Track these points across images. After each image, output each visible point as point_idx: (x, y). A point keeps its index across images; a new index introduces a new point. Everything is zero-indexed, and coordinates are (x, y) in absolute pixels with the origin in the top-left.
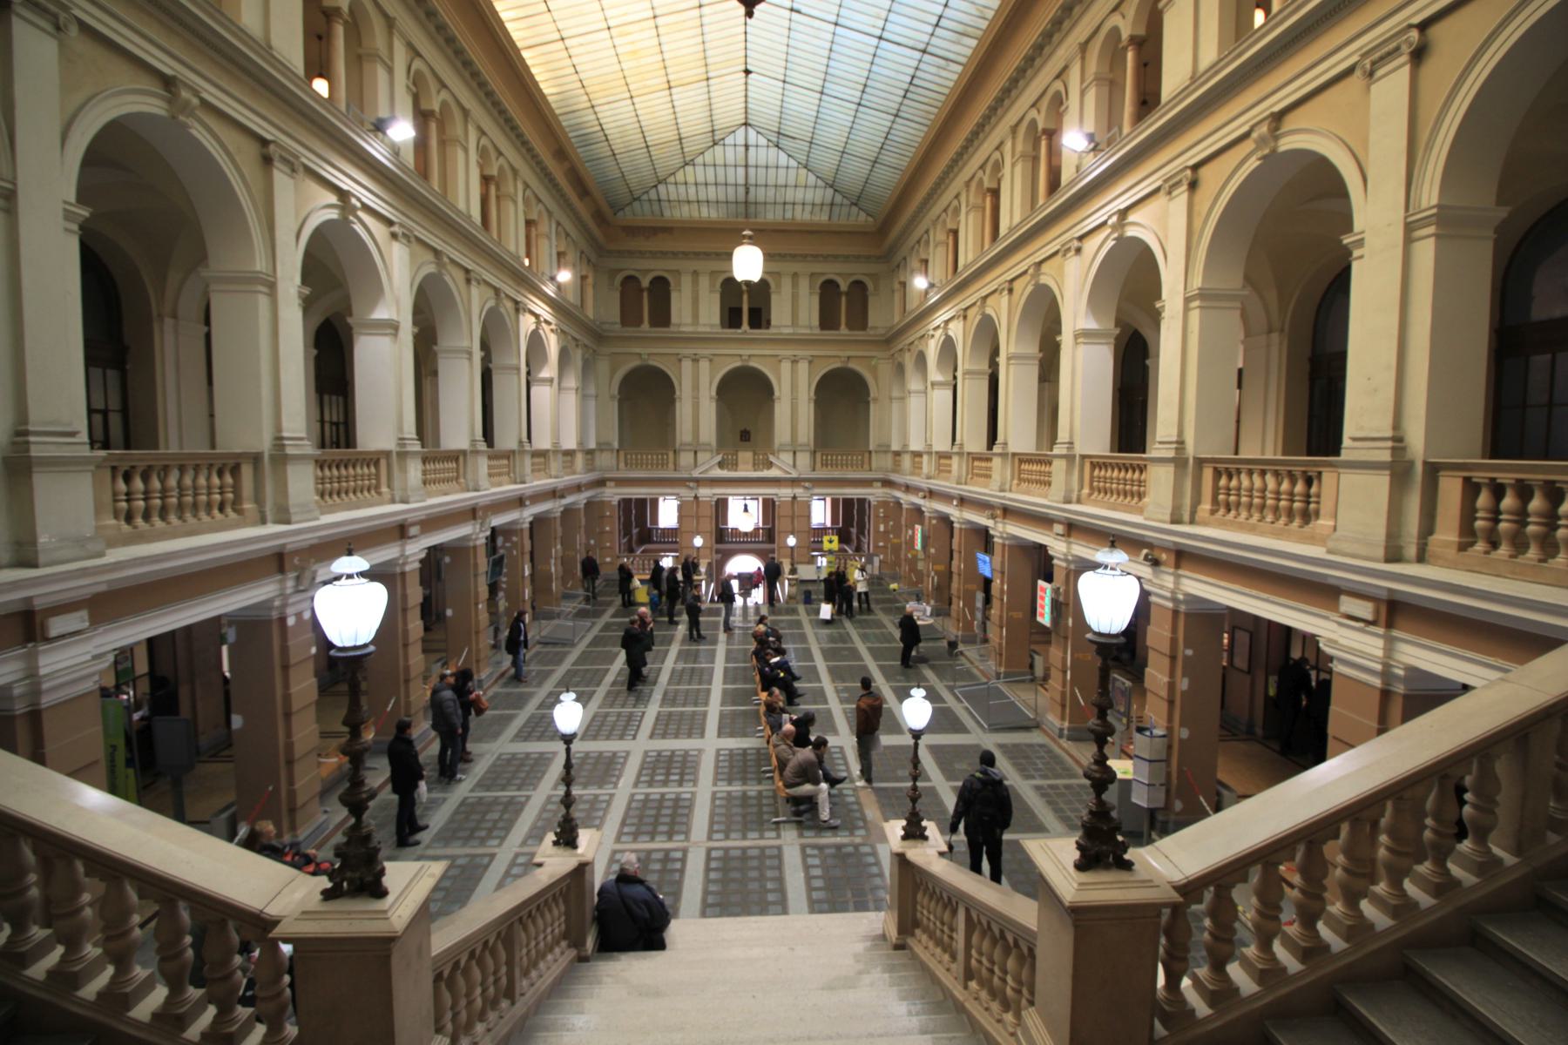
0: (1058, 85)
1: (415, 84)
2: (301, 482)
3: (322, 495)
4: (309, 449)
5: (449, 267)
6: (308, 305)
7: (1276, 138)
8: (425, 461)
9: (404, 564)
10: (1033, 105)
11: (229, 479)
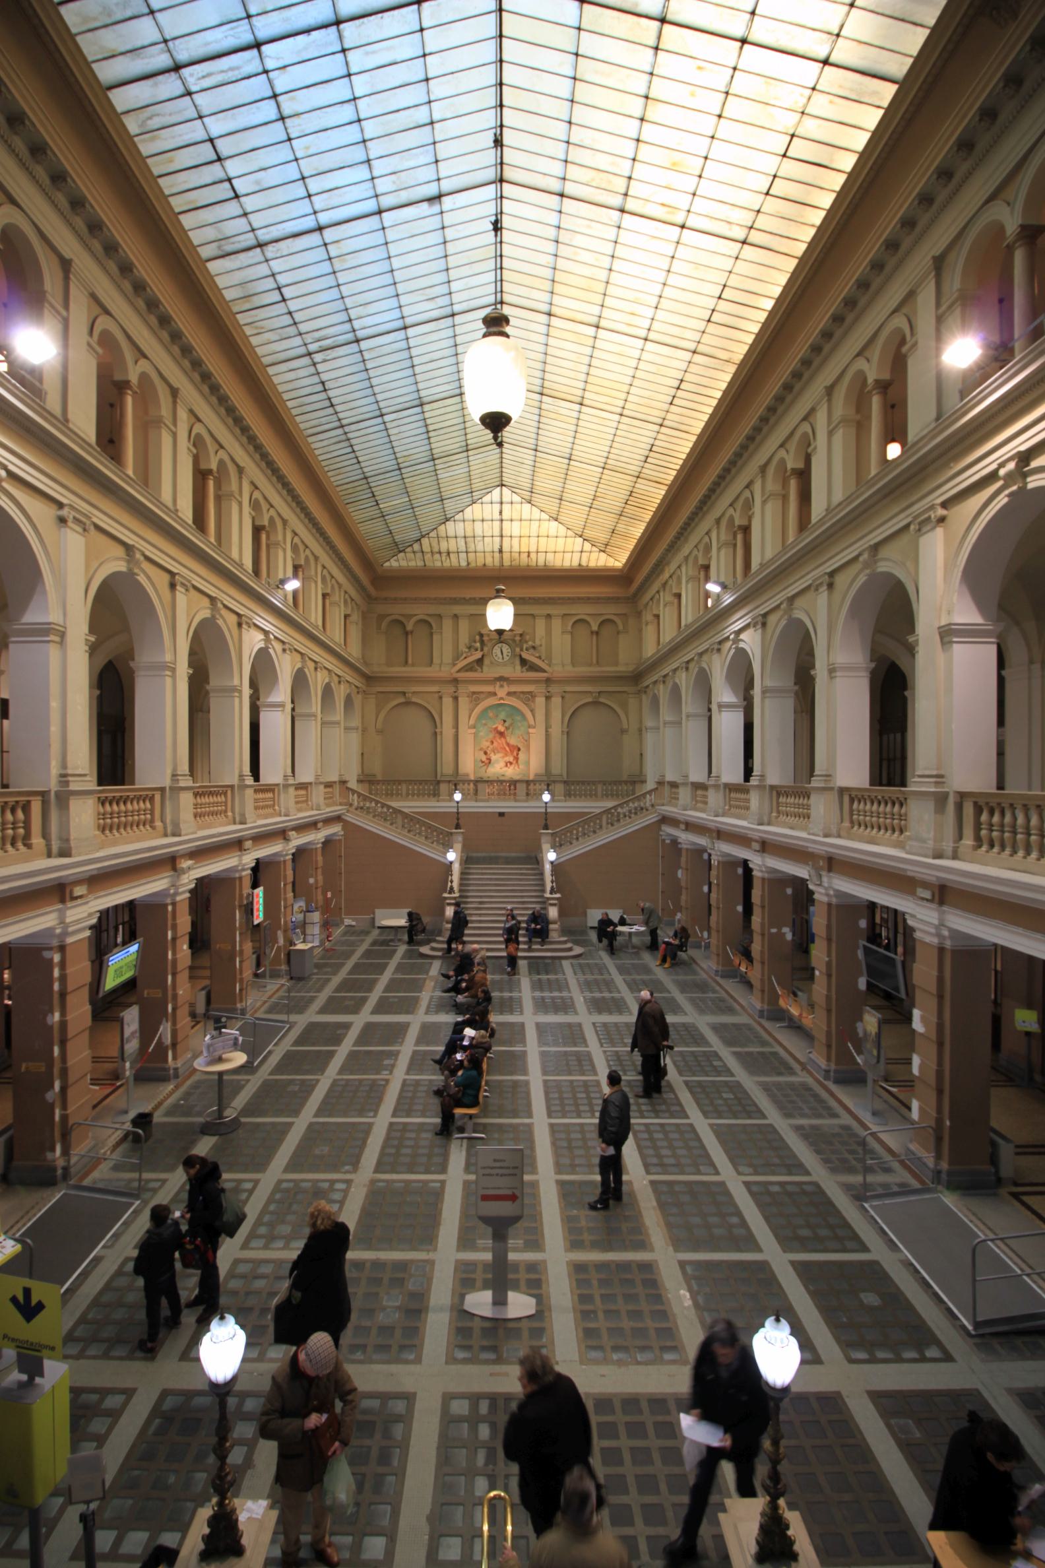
0: (900, 322)
1: (194, 445)
2: (83, 815)
3: (103, 831)
4: (91, 784)
5: (224, 612)
6: (93, 650)
7: (1025, 476)
8: (196, 795)
9: (176, 894)
10: (782, 446)
11: (20, 815)
